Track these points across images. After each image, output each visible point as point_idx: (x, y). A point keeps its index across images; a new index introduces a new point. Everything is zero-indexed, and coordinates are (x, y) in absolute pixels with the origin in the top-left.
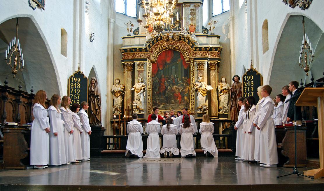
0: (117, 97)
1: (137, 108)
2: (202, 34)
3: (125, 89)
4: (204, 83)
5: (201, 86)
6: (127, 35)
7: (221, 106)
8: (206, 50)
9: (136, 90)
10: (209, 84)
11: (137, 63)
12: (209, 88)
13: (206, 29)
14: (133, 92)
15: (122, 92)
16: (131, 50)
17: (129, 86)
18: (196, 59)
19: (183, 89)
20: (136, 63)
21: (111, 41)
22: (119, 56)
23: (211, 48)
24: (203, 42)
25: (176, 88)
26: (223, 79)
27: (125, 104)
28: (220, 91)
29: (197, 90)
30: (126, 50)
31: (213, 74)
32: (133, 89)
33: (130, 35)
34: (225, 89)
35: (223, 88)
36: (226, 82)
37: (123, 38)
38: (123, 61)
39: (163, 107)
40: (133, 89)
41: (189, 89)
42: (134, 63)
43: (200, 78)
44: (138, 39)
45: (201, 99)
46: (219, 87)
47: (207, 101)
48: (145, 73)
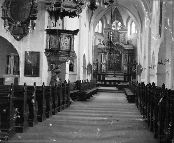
0: (95, 65)
1: (103, 70)
2: (126, 44)
13: (129, 42)
18: (124, 53)
21: (94, 45)
24: (127, 47)
37: (98, 44)
40: (102, 63)
48: (106, 57)
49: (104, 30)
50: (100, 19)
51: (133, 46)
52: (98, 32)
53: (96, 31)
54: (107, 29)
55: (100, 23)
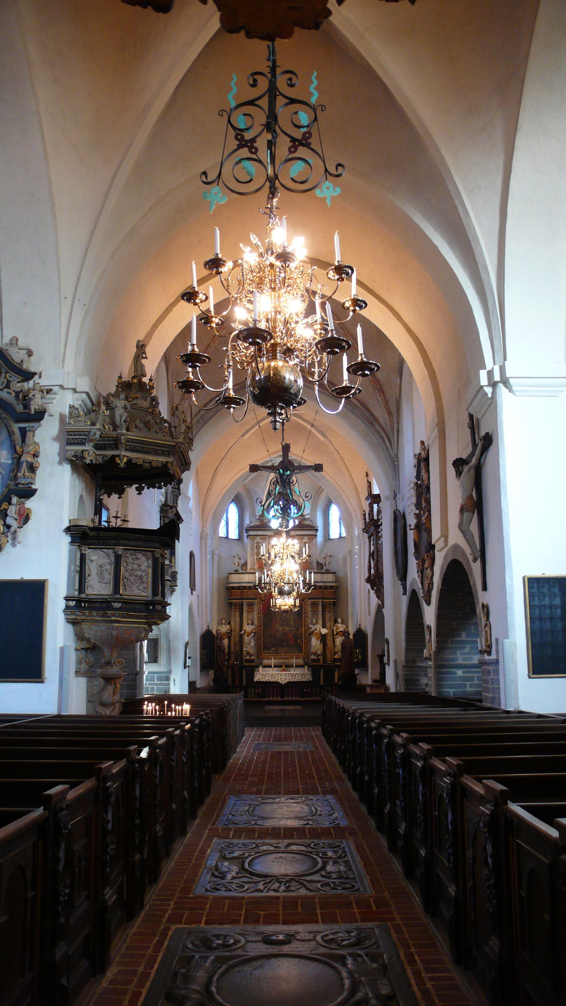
1: (248, 653)
3: (231, 630)
4: (319, 625)
5: (316, 629)
6: (235, 571)
7: (337, 649)
8: (320, 589)
9: (246, 634)
10: (324, 626)
11: (245, 602)
12: (324, 631)
14: (241, 636)
15: (228, 633)
16: (239, 588)
17: (237, 627)
18: (309, 599)
19: (296, 631)
20: (244, 603)
21: (216, 576)
23: (326, 587)
25: (289, 630)
26: (339, 620)
27: (232, 646)
28: (335, 633)
29: (311, 633)
30: (233, 588)
31: (327, 616)
32: (243, 632)
33: (237, 571)
34: (341, 631)
35: (339, 630)
36: (342, 623)
38: (229, 599)
39: (275, 651)
41: (302, 631)
42: (243, 602)
43: (314, 620)
44: (247, 575)
45: (315, 643)
46: (335, 629)
47: (322, 645)
49: (247, 531)
50: (233, 496)
52: (227, 537)
53: (222, 533)
55: (233, 510)
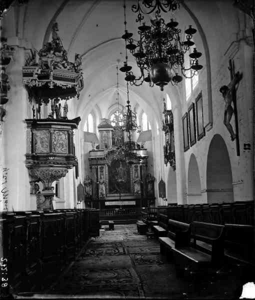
16: (95, 159)
22: (88, 162)
28: (147, 181)
32: (98, 183)
37: (91, 151)
40: (98, 183)
51: (147, 152)
54: (103, 125)
